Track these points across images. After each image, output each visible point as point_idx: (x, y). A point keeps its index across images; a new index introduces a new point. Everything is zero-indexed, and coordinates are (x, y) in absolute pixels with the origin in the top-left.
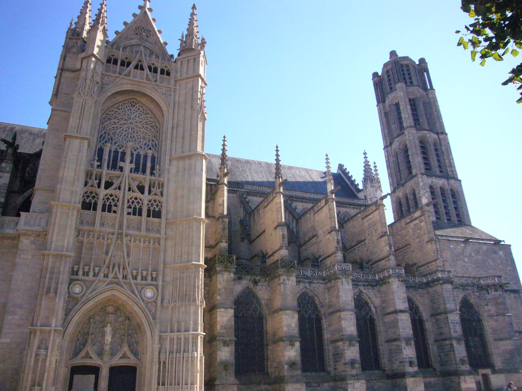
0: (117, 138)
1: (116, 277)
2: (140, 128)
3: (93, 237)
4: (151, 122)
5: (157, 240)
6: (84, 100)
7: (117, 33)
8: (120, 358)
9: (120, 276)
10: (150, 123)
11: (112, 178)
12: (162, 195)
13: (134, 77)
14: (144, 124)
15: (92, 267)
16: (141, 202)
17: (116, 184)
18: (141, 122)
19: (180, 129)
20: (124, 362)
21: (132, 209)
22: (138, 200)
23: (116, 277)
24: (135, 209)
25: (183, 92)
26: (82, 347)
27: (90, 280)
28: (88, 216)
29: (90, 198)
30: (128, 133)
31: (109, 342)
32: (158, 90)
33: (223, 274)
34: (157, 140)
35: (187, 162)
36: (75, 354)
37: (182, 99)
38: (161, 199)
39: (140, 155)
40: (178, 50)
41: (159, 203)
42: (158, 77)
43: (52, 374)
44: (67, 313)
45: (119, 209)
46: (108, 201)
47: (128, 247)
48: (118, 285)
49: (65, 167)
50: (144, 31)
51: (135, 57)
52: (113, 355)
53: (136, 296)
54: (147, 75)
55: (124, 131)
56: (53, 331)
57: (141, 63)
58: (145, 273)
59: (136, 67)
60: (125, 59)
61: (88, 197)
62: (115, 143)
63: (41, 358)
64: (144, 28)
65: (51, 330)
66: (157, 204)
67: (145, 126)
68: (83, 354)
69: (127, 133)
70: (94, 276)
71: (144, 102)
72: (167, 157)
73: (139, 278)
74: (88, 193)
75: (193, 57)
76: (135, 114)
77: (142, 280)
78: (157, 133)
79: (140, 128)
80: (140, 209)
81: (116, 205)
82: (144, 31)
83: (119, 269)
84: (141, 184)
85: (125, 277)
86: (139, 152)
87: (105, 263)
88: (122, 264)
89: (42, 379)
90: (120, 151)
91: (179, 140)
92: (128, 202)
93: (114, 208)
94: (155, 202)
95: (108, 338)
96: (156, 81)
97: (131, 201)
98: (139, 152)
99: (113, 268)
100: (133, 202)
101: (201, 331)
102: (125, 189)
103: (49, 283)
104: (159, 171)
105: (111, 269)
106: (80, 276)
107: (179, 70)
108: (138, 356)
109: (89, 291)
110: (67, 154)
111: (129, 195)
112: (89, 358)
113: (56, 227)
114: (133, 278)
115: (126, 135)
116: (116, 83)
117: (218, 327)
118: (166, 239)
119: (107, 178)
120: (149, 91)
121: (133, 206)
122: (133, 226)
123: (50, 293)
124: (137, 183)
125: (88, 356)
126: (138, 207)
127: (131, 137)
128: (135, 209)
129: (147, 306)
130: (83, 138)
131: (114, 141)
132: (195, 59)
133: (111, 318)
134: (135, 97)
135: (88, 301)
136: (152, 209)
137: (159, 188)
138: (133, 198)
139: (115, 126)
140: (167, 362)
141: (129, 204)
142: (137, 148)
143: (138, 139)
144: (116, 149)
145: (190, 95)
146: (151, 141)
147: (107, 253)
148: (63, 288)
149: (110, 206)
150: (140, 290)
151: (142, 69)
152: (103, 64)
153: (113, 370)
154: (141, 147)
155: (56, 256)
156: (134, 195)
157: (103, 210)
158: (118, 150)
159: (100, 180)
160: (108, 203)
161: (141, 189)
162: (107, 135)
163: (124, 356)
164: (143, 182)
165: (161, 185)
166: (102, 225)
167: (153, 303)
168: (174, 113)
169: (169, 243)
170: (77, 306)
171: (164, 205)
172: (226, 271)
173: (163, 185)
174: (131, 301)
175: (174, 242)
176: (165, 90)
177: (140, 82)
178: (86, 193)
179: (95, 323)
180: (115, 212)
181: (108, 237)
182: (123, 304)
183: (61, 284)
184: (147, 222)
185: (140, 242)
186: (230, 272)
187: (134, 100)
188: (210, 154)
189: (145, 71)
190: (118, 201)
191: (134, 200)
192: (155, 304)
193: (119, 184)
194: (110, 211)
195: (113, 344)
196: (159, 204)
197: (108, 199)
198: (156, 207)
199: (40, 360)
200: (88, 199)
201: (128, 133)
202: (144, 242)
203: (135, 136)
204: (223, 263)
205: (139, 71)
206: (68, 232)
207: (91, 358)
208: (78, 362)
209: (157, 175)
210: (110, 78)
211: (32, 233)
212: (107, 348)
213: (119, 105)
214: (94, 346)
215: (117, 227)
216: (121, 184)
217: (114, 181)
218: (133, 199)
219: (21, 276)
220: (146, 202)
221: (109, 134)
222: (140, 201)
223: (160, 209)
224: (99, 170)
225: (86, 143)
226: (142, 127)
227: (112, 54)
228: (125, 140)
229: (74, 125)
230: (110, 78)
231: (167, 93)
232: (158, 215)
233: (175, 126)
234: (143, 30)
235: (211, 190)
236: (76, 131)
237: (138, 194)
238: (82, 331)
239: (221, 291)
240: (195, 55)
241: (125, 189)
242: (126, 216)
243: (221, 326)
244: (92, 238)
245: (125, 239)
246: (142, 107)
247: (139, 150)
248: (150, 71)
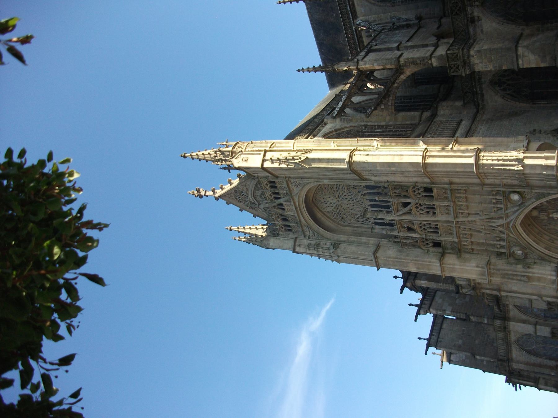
9: (501, 222)
22: (418, 206)
23: (502, 226)
33: (474, 65)
55: (348, 200)
57: (276, 206)
60: (280, 218)
61: (427, 244)
64: (235, 195)
81: (430, 224)
85: (501, 218)
87: (489, 233)
97: (421, 212)
101: (555, 153)
115: (351, 200)
117: (542, 65)
134: (311, 201)
152: (296, 238)
155: (490, 275)
156: (414, 210)
160: (429, 230)
172: (470, 62)
185: (462, 205)
186: (469, 56)
187: (314, 200)
204: (457, 55)
218: (418, 210)
221: (358, 218)
231: (294, 184)
232: (429, 190)
239: (495, 65)
243: (542, 62)
245: (461, 219)
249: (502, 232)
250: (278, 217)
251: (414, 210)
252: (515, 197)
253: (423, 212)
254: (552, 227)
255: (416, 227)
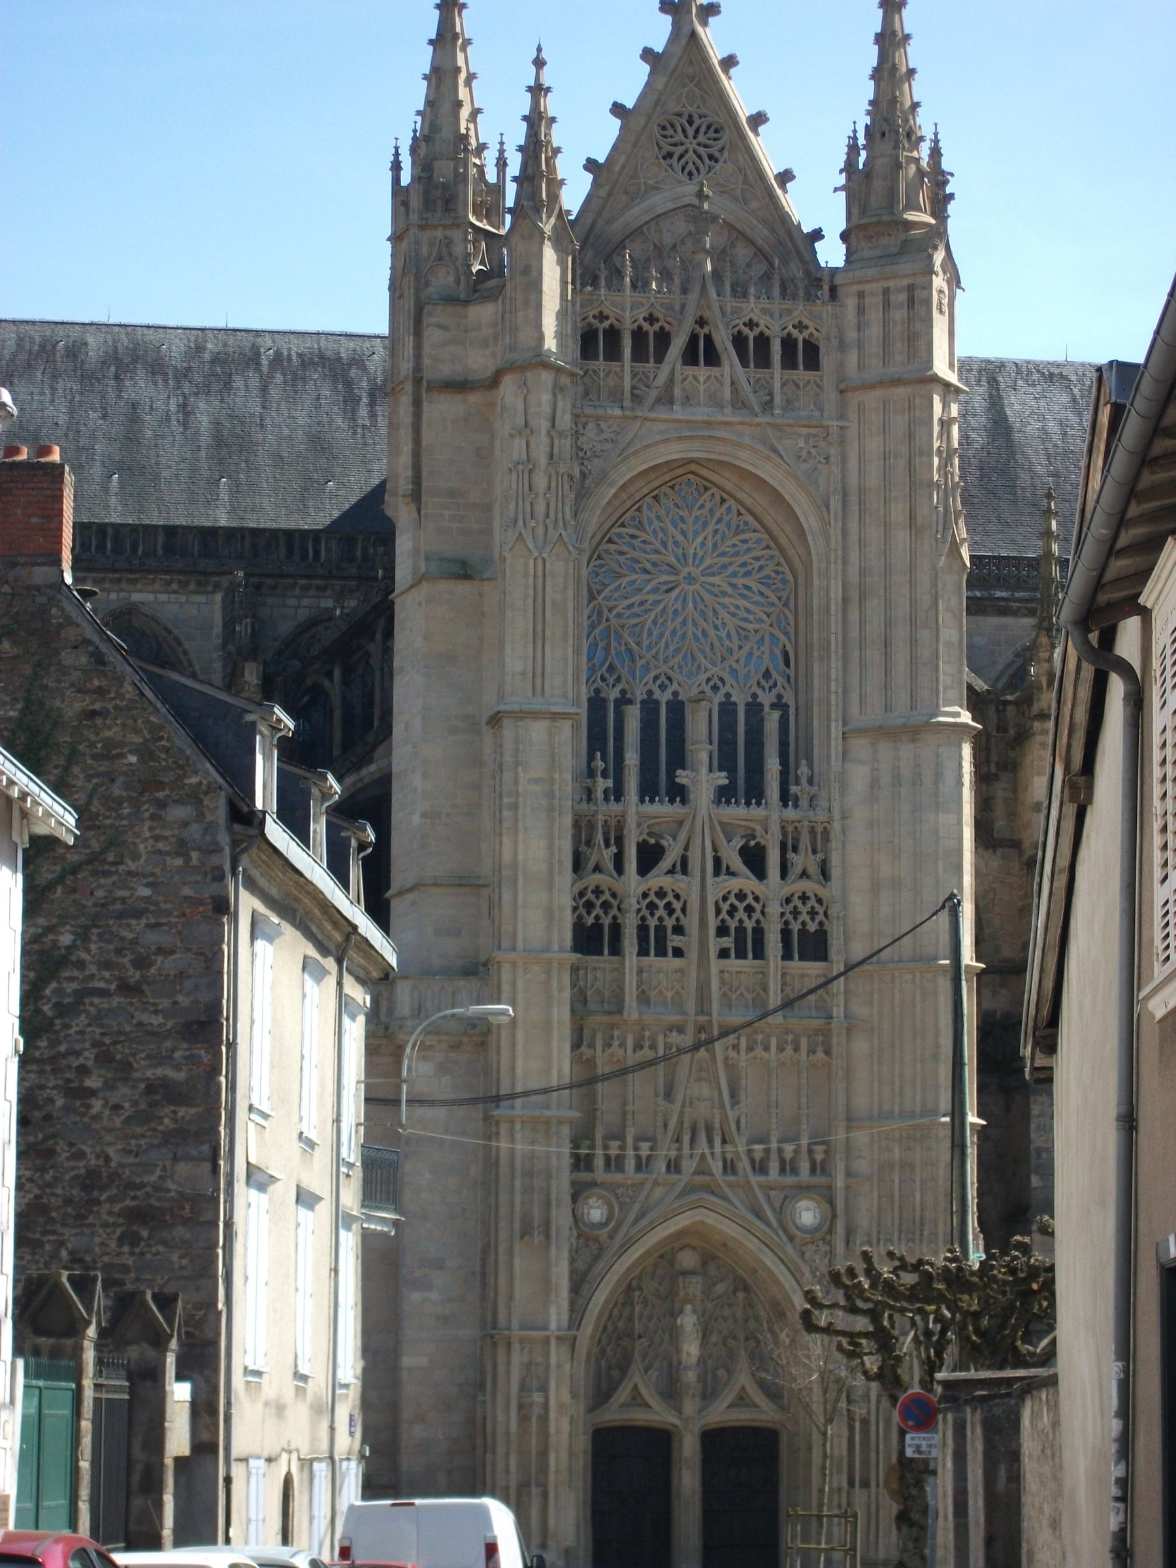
0: (650, 647)
1: (702, 1170)
2: (725, 594)
3: (622, 1045)
4: (762, 562)
5: (821, 1039)
6: (540, 562)
7: (591, 165)
8: (729, 1407)
9: (717, 1166)
10: (757, 564)
11: (656, 829)
12: (825, 873)
13: (687, 400)
14: (734, 574)
15: (630, 1141)
16: (758, 907)
17: (671, 857)
18: (724, 566)
19: (874, 605)
20: (741, 1417)
21: (732, 939)
23: (702, 1170)
24: (741, 930)
25: (874, 445)
26: (616, 1374)
27: (630, 1182)
28: (599, 974)
29: (598, 911)
30: (684, 623)
31: (694, 1360)
32: (779, 447)
34: (786, 633)
35: (906, 751)
36: (601, 1394)
37: (874, 478)
38: (823, 893)
39: (735, 704)
40: (836, 190)
41: (816, 905)
42: (777, 385)
43: (564, 1454)
44: (579, 1284)
45: (690, 942)
46: (652, 914)
47: (730, 1066)
48: (713, 1193)
49: (515, 829)
50: (697, 131)
51: (683, 306)
52: (708, 1394)
53: (769, 1225)
54: (733, 383)
56: (553, 1341)
57: (706, 330)
58: (789, 1149)
59: (690, 357)
61: (589, 906)
62: (646, 668)
63: (536, 1411)
64: (697, 122)
65: (548, 1338)
66: (813, 908)
67: (740, 581)
68: (623, 1394)
69: (679, 620)
70: (639, 1168)
71: (728, 486)
72: (833, 725)
73: (774, 1166)
74: (590, 896)
75: (905, 282)
76: (700, 539)
77: (782, 1171)
78: (786, 605)
79: (725, 594)
80: (759, 932)
81: (679, 930)
82: (697, 131)
83: (710, 1141)
84: (752, 843)
85: (729, 1167)
86: (728, 695)
87: (665, 1125)
88: (717, 1125)
89: (544, 1469)
90: (664, 697)
91: (874, 655)
92: (718, 911)
93: (674, 941)
94: (804, 904)
95: (691, 1349)
96: (768, 405)
97: (725, 907)
98: (728, 695)
99: (693, 1141)
100: (732, 910)
102: (703, 871)
103: (523, 1203)
104: (810, 781)
105: (686, 1150)
106: (600, 1173)
107: (852, 335)
108: (781, 1397)
109: (631, 1217)
110: (516, 782)
111: (718, 886)
112: (640, 1405)
113: (520, 1034)
114: (754, 1168)
116: (629, 444)
118: (849, 1031)
119: (641, 833)
120: (744, 454)
121: (733, 924)
122: (741, 994)
123: (532, 1235)
124: (738, 843)
125: (636, 1400)
126: (749, 925)
127: (697, 639)
128: (741, 930)
129: (803, 1254)
130: (555, 717)
131: (640, 663)
132: (911, 288)
133: (695, 1286)
135: (627, 1246)
136: (795, 927)
137: (814, 852)
138: (733, 896)
139: (636, 599)
140: (873, 1419)
141: (720, 918)
142: (722, 680)
143: (720, 639)
144: (650, 693)
145: (902, 462)
146: (767, 638)
147: (669, 1095)
148: (562, 1218)
149: (660, 929)
150: (777, 1205)
151: (712, 358)
153: (712, 1439)
154: (733, 671)
156: (735, 884)
157: (643, 952)
158: (657, 694)
159: (620, 842)
160: (652, 923)
161: (754, 859)
162: (613, 644)
163: (741, 1400)
164: (758, 834)
165: (821, 838)
166: (644, 999)
167: (821, 1243)
168: (845, 533)
169: (861, 1046)
170: (601, 1264)
171: (834, 911)
173: (826, 833)
174: (755, 1240)
175: (876, 1043)
176: (806, 442)
177: (709, 424)
178: (582, 894)
179: (645, 1302)
180: (678, 952)
181: (668, 1040)
182: (725, 1245)
183: (558, 1206)
184: (783, 975)
185: (767, 1049)
188: (1001, 365)
189: (726, 370)
190: (684, 910)
191: (736, 903)
192: (827, 1248)
193: (682, 852)
194: (661, 952)
195: (705, 1362)
196: (818, 908)
197: (652, 907)
198: (807, 918)
199: (534, 1420)
200: (589, 913)
201: (684, 623)
202: (781, 1049)
203: (712, 632)
205: (702, 372)
206: (555, 1045)
207: (648, 1406)
208: (616, 1417)
209: (804, 802)
210: (602, 423)
211: (439, 1041)
212: (690, 1377)
213: (638, 510)
214: (650, 1372)
215: (691, 1006)
216: (686, 849)
217: (664, 843)
218: (732, 899)
219: (428, 1176)
220: (774, 909)
221: (619, 637)
222: (754, 904)
223: (821, 924)
224: (614, 807)
225: (566, 726)
226: (730, 590)
227: (596, 312)
228: (678, 650)
229: (519, 667)
230: (604, 425)
231: (813, 451)
233: (854, 595)
234: (691, 131)
235: (1002, 728)
236: (529, 692)
237: (746, 882)
238: (610, 1328)
240: (914, 275)
241: (703, 871)
242: (715, 965)
244: (620, 1046)
246: (723, 501)
247: (727, 688)
248: (744, 363)
249: (674, 1166)
250: (651, 319)
251: (735, 884)
252: (807, 1214)
253: (724, 915)
254: (638, 1309)
255: (658, 879)
